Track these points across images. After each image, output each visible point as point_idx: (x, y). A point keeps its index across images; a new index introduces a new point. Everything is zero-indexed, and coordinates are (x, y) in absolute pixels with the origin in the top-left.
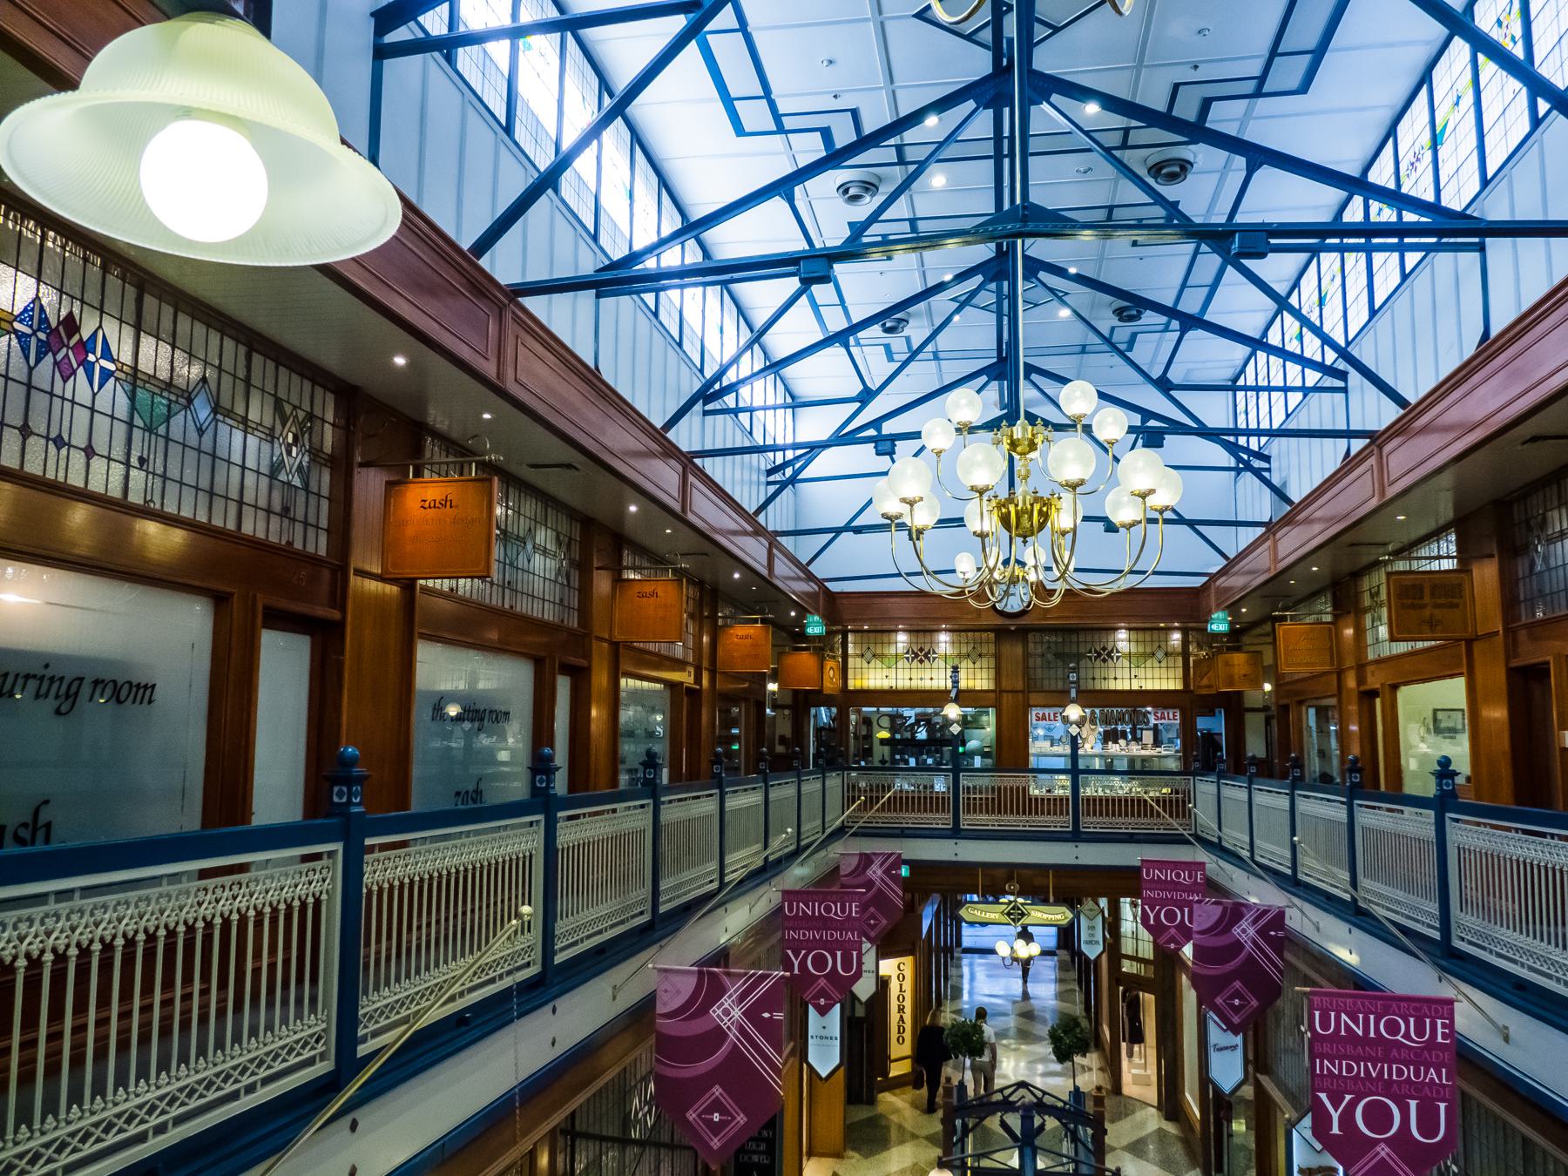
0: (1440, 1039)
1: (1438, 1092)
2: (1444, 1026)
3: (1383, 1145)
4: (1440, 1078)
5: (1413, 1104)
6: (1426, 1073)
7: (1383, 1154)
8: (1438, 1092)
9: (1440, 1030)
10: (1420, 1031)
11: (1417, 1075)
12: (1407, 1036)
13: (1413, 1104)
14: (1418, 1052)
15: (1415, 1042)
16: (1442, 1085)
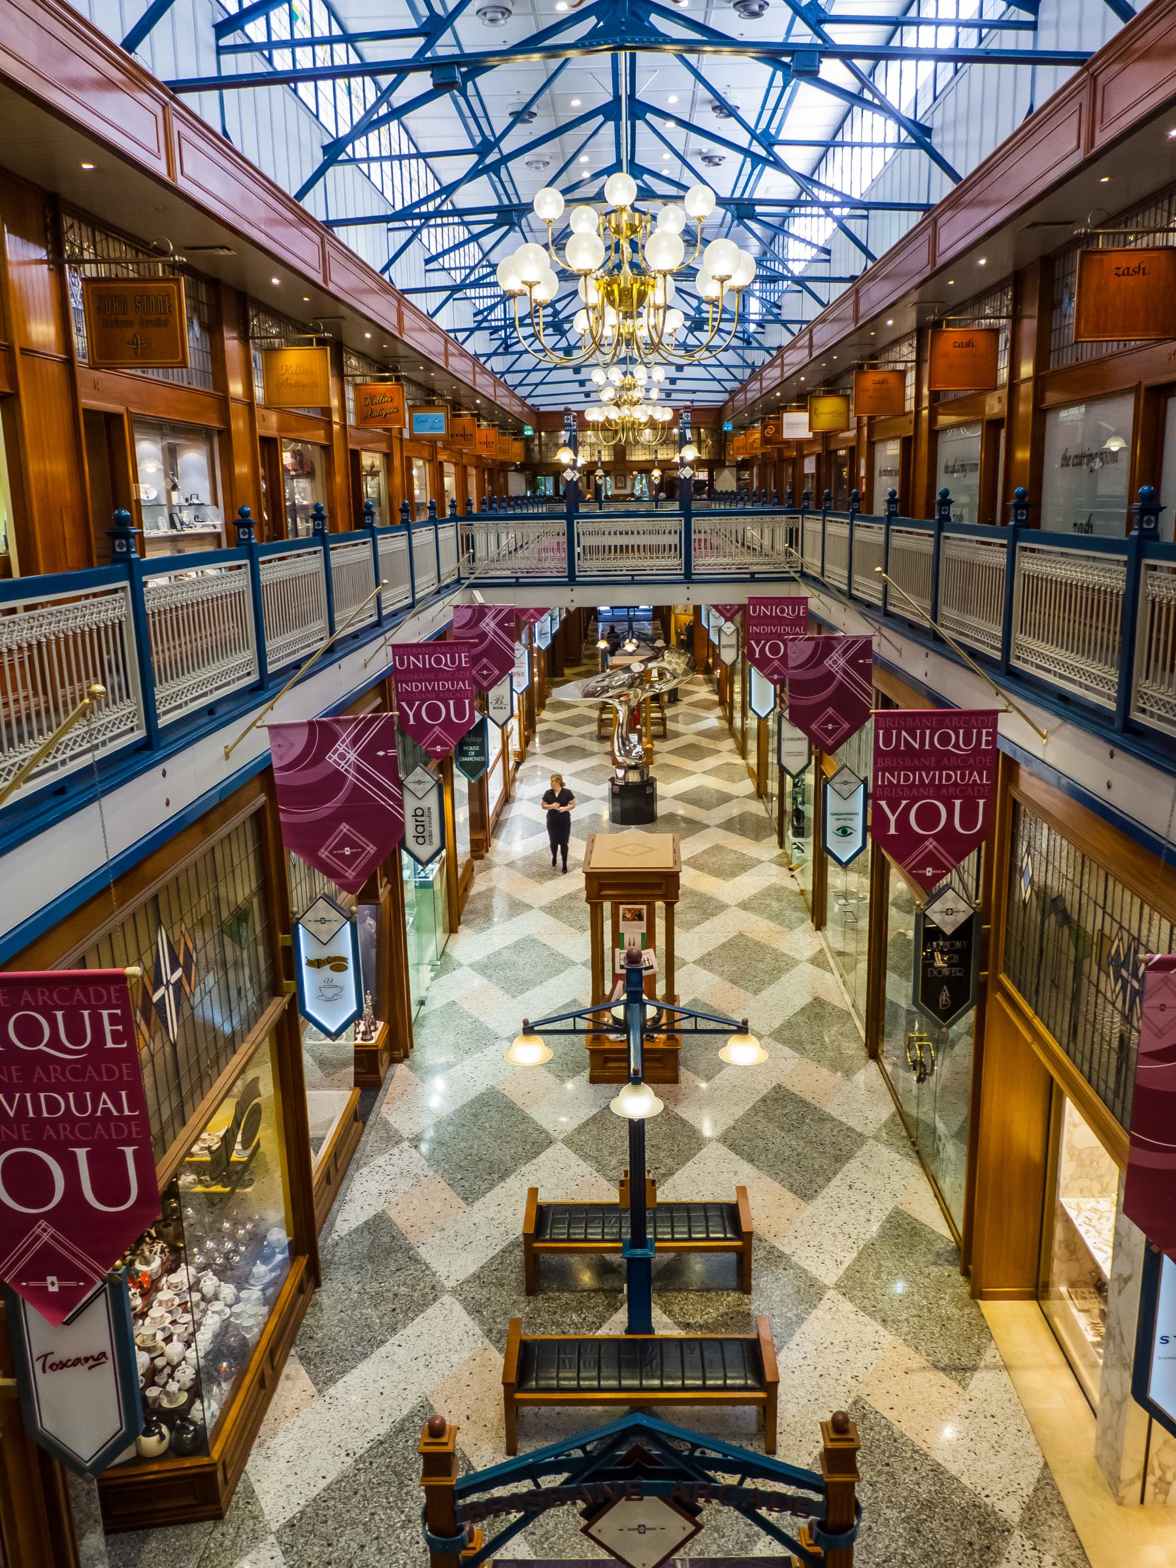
0: (110, 1044)
1: (119, 1131)
2: (113, 1019)
3: (43, 1224)
4: (119, 1108)
5: (81, 1153)
6: (96, 1101)
7: (46, 1237)
8: (119, 1131)
9: (108, 1028)
10: (76, 1034)
11: (81, 1107)
12: (55, 1042)
13: (81, 1153)
14: (77, 1069)
15: (70, 1053)
16: (122, 1118)
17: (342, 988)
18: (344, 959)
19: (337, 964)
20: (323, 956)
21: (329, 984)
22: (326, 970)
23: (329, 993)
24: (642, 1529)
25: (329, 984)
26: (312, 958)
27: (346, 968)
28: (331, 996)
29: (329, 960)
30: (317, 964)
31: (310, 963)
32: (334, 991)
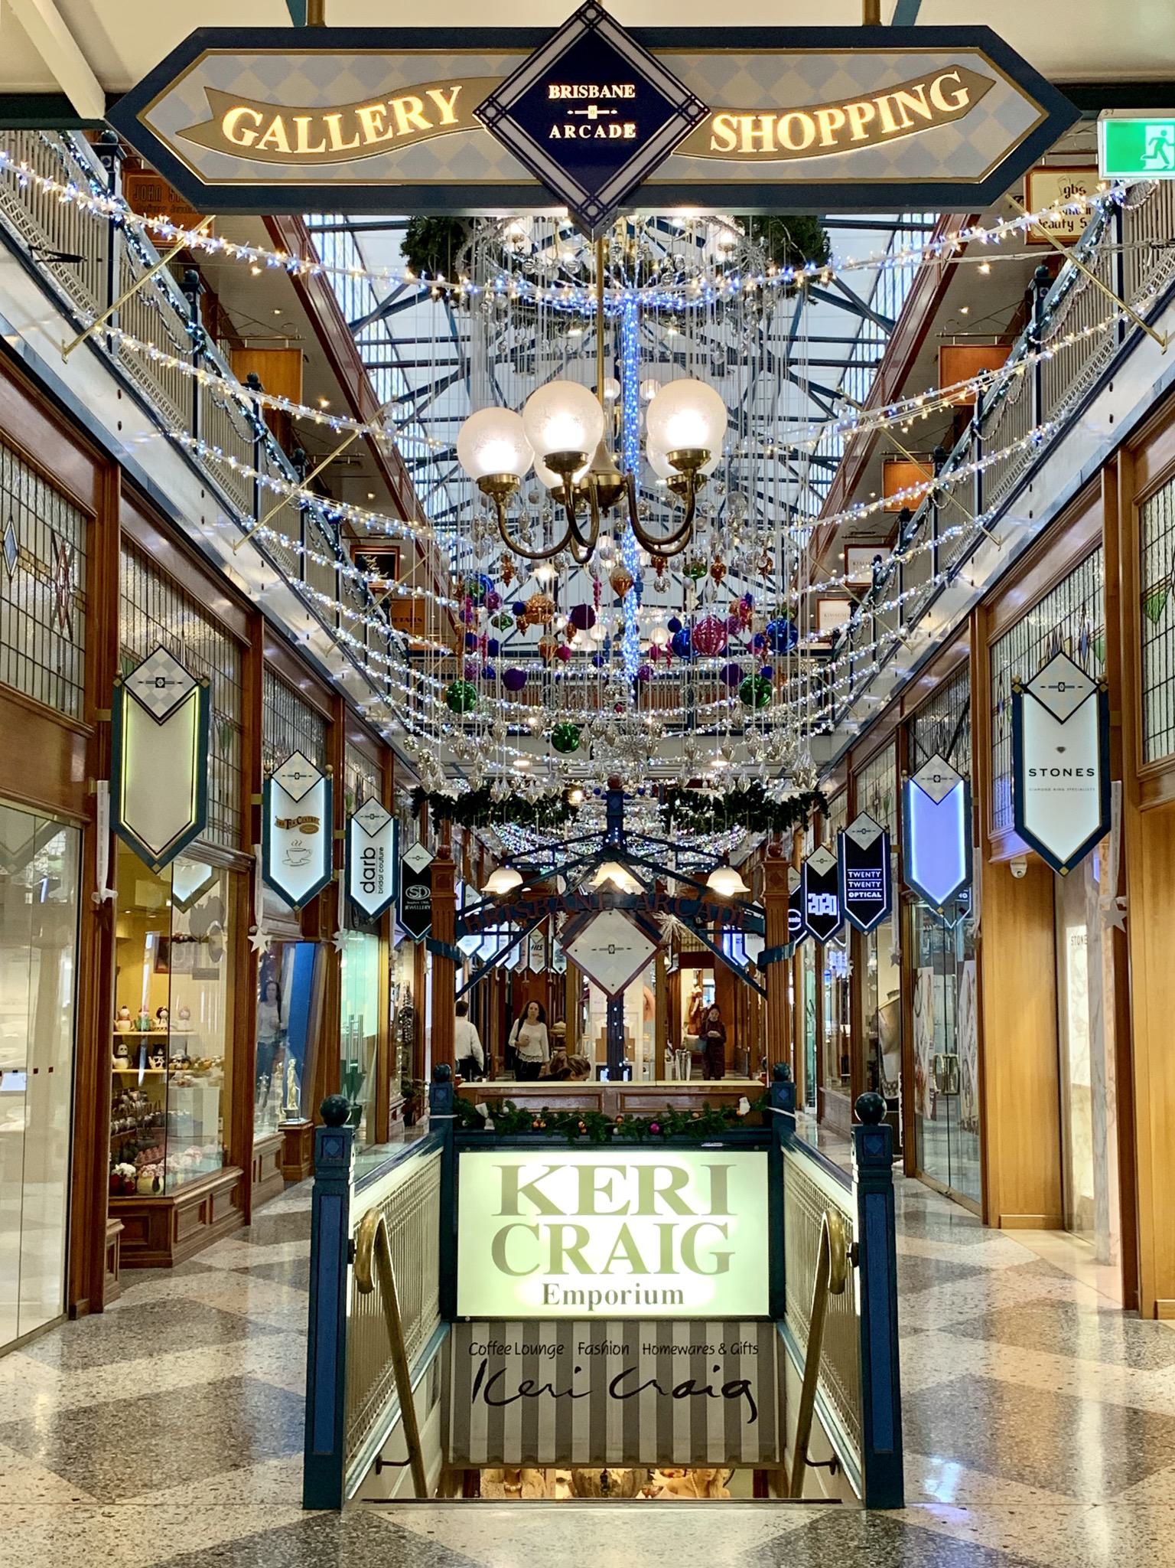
17: (310, 852)
18: (315, 820)
19: (307, 825)
20: (294, 817)
21: (298, 848)
22: (296, 833)
23: (296, 857)
24: (612, 949)
25: (298, 848)
26: (282, 818)
27: (317, 829)
28: (298, 858)
29: (299, 821)
30: (286, 824)
31: (279, 823)
32: (302, 854)
